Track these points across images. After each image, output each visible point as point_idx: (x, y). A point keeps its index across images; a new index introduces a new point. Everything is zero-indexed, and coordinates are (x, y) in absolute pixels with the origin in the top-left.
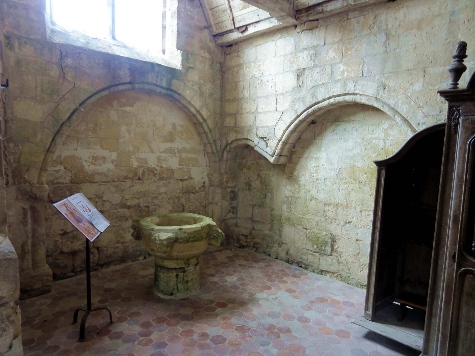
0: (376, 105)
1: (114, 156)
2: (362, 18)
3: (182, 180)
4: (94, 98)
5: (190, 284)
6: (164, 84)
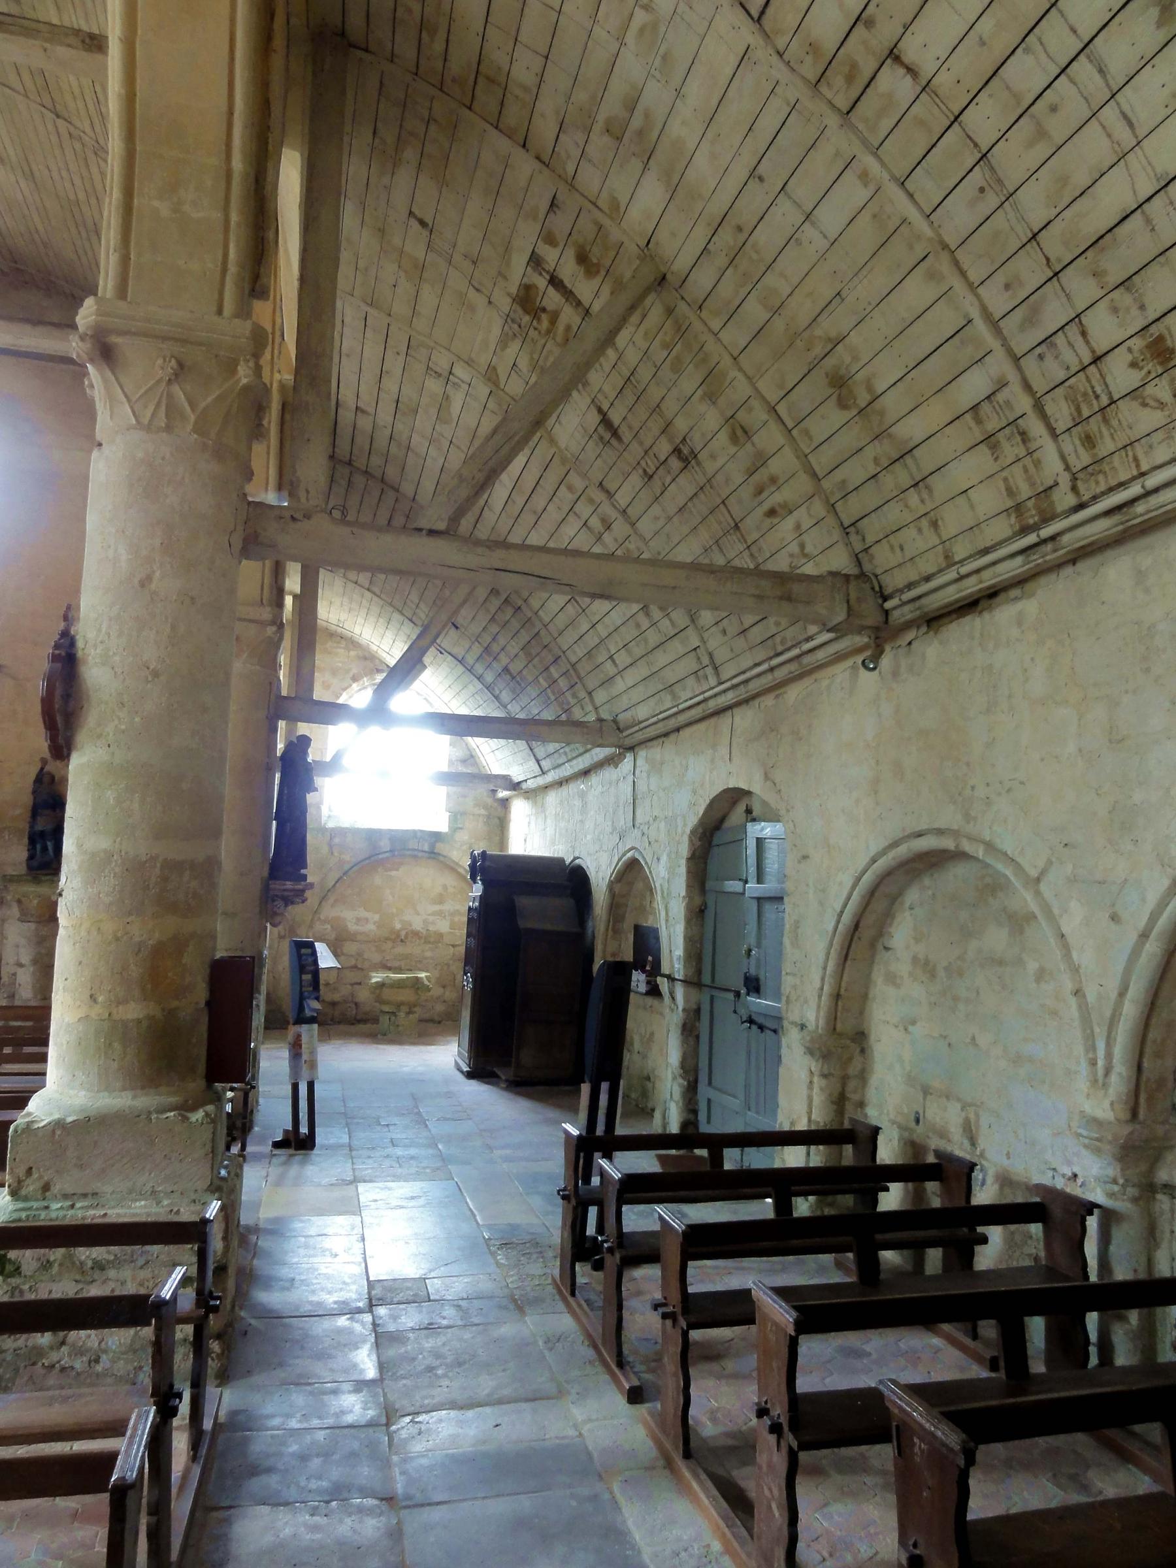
1: (377, 917)
3: (453, 946)
4: (356, 868)
5: (401, 1028)
6: (426, 848)
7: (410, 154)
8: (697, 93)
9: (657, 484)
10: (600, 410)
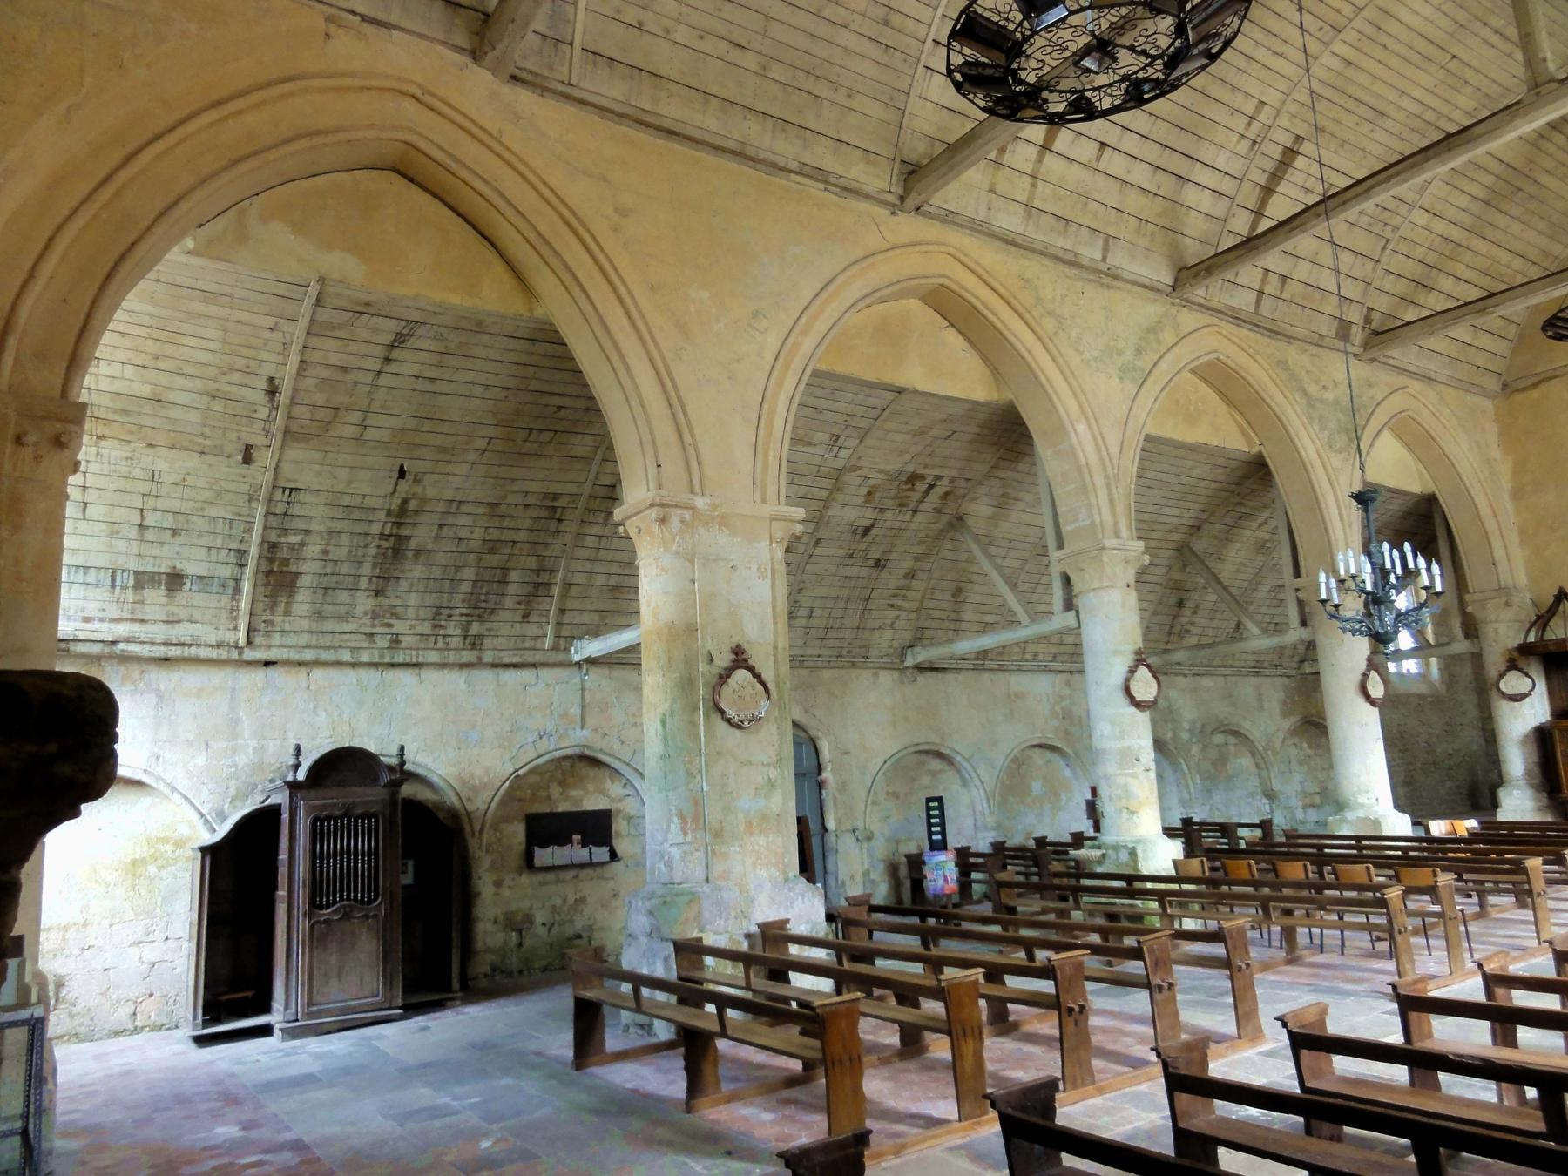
0: (145, 779)
2: (122, 669)
7: (986, 432)
8: (1026, 518)
9: (851, 561)
10: (873, 525)
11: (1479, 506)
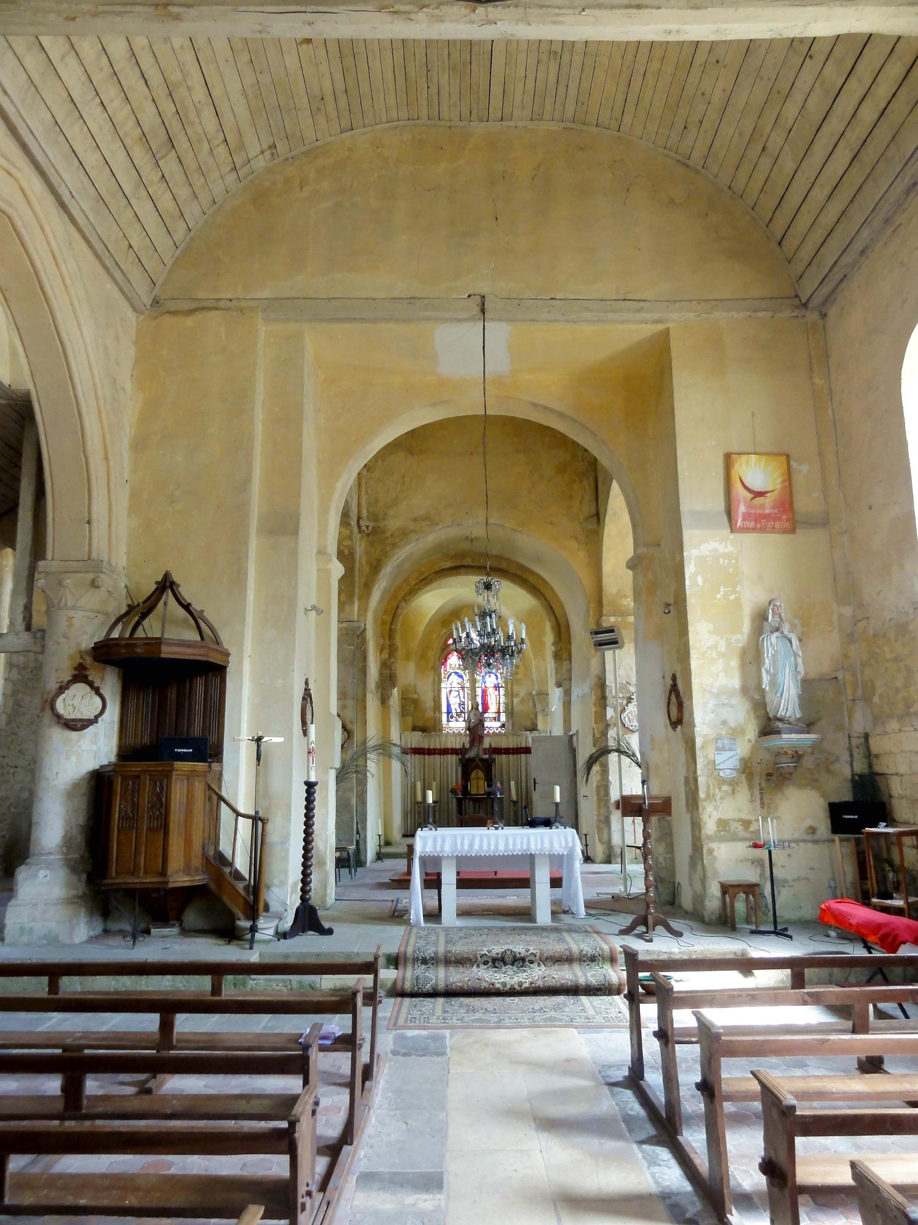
11: (88, 433)
